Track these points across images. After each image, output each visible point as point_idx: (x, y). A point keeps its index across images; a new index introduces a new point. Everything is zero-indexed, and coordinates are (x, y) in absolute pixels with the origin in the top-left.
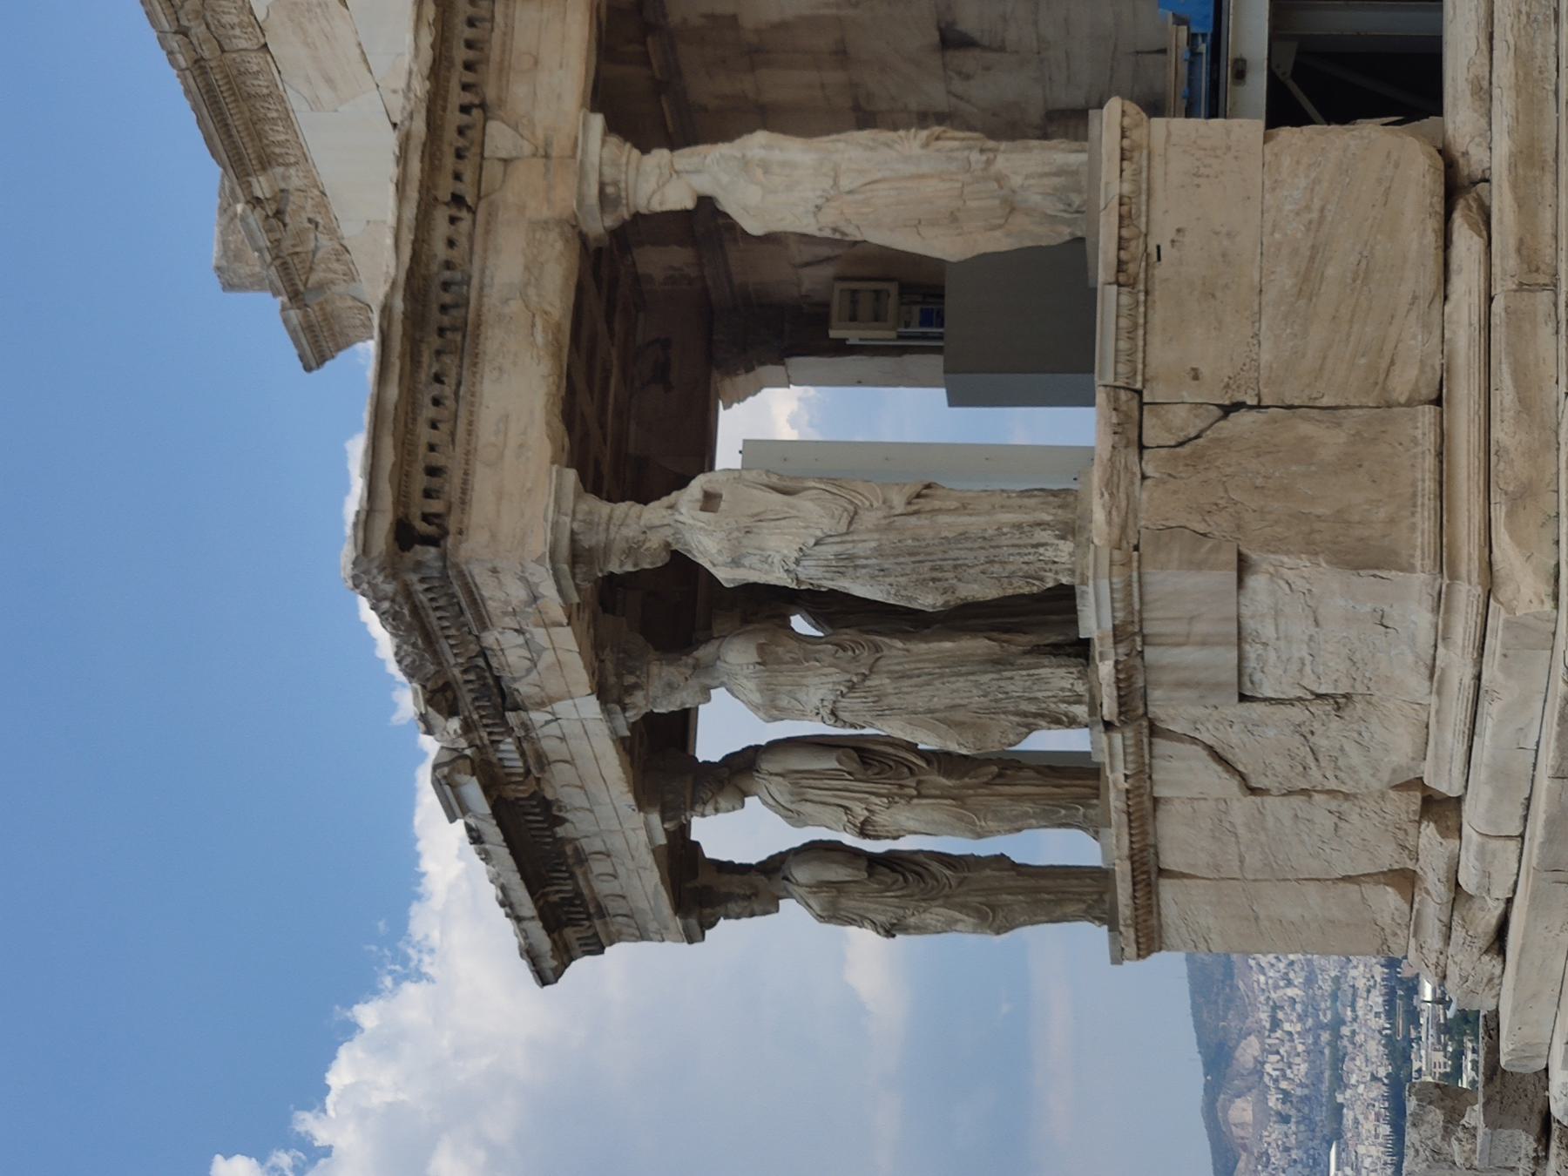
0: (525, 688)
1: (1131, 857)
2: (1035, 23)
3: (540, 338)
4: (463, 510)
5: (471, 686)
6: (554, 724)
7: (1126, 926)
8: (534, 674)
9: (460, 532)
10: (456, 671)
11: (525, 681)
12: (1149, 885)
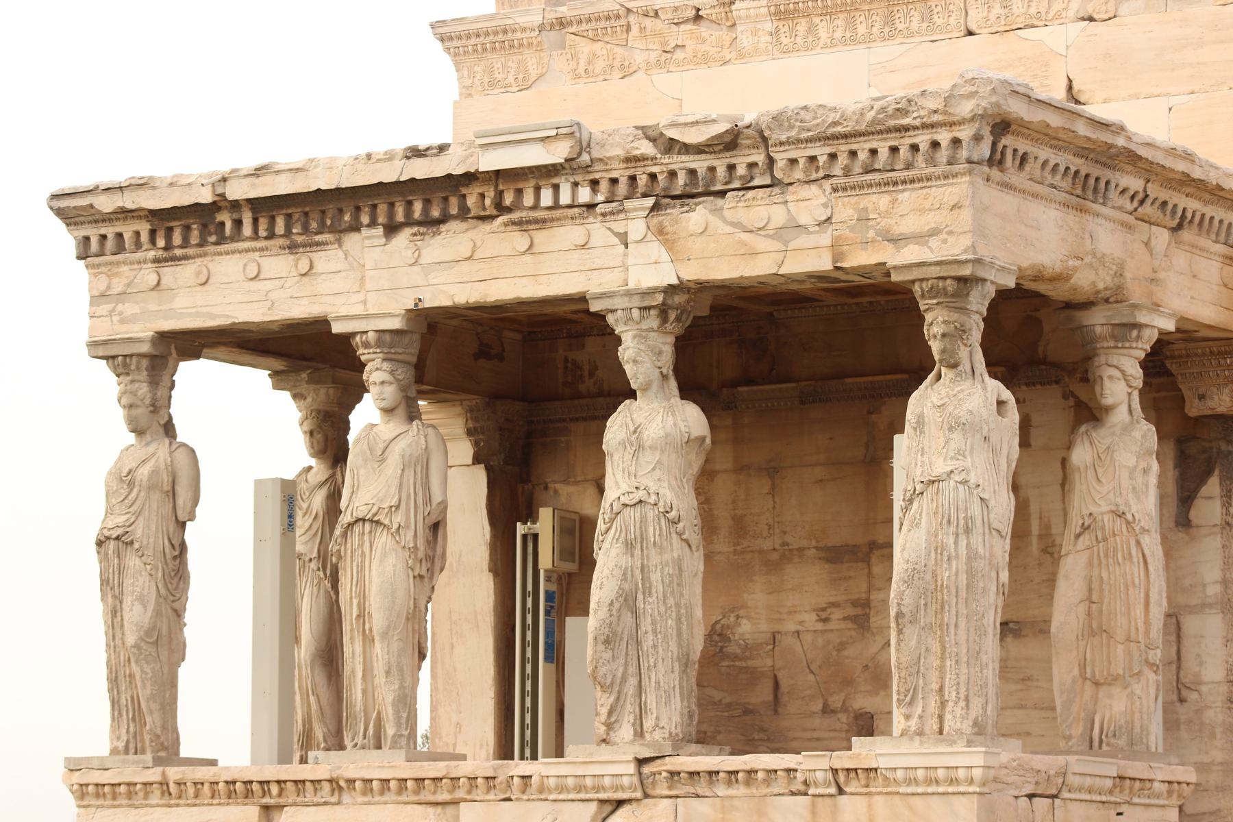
0: (698, 216)
1: (330, 781)
2: (1021, 707)
3: (1071, 263)
4: (998, 183)
5: (721, 172)
6: (616, 241)
7: (164, 773)
8: (729, 229)
9: (988, 180)
10: (759, 158)
11: (714, 221)
12: (248, 794)
